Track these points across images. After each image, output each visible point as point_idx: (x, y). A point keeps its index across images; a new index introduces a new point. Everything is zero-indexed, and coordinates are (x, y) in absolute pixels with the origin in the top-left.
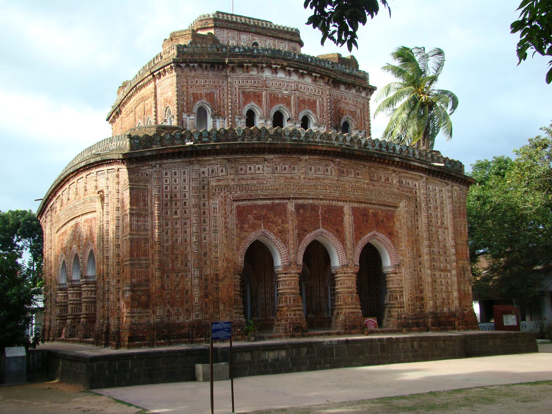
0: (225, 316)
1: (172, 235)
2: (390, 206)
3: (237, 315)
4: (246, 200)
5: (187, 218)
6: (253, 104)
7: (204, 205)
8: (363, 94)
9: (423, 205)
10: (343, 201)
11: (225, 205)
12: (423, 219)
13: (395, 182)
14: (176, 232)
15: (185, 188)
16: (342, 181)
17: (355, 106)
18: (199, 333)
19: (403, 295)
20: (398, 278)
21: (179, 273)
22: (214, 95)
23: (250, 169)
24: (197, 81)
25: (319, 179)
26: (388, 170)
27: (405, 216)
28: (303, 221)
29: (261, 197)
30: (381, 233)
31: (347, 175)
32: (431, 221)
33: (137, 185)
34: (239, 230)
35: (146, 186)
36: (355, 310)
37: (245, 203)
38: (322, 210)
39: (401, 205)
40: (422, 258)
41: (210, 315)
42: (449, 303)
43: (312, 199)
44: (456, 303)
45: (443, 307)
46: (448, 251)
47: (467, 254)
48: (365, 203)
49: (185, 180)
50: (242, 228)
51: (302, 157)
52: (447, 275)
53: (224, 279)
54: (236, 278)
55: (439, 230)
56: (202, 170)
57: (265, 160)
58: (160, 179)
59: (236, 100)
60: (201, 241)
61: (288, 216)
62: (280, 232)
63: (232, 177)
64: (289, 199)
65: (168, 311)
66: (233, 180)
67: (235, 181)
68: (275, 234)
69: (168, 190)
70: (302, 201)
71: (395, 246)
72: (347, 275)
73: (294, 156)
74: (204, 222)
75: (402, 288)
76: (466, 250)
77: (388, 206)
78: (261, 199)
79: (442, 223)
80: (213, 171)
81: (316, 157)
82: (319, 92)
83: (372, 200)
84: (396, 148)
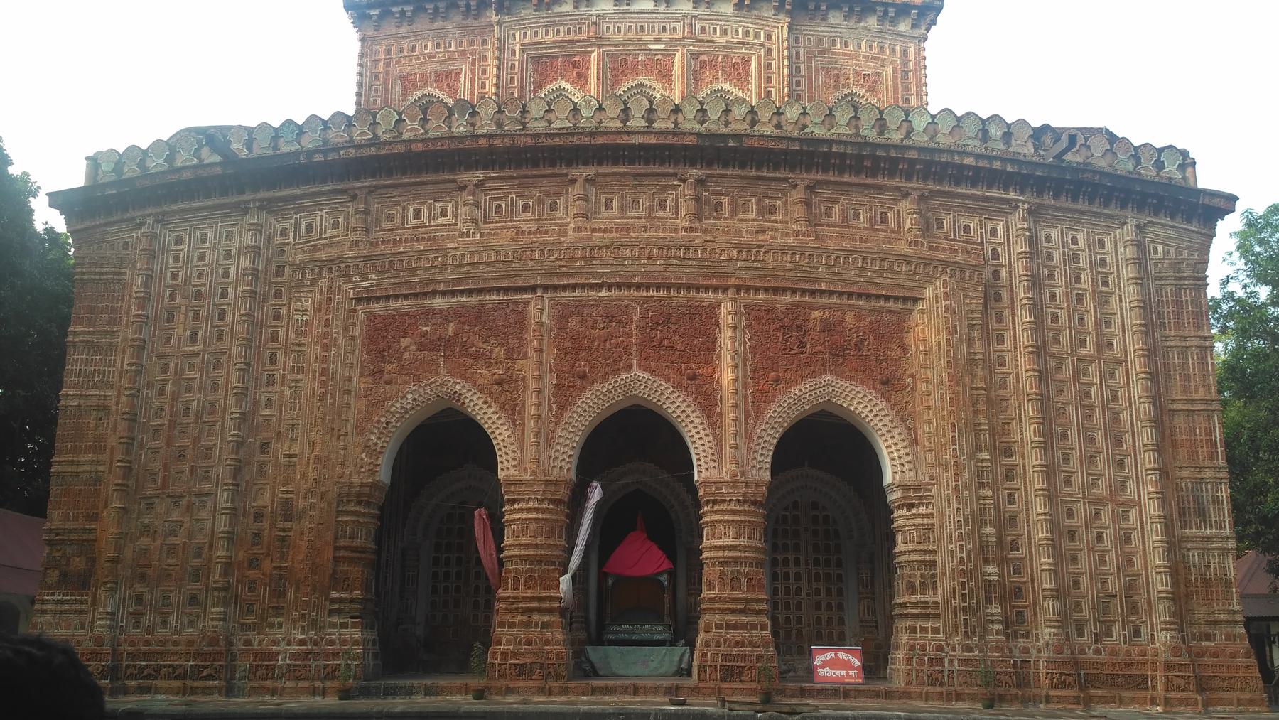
0: (296, 621)
1: (173, 399)
2: (887, 298)
3: (336, 619)
4: (397, 297)
5: (223, 353)
6: (562, 83)
7: (277, 317)
8: (903, 27)
9: (1020, 292)
10: (716, 289)
11: (328, 311)
12: (1019, 336)
13: (908, 225)
14: (188, 390)
15: (226, 274)
16: (706, 231)
17: (874, 59)
18: (205, 667)
19: (934, 576)
20: (919, 521)
21: (181, 496)
22: (458, 74)
23: (418, 214)
24: (414, 47)
25: (627, 229)
26: (880, 189)
27: (942, 325)
28: (576, 350)
29: (441, 287)
30: (852, 379)
31: (733, 213)
32: (1056, 340)
33: (96, 273)
34: (369, 379)
35: (120, 273)
36: (743, 619)
37: (393, 304)
38: (643, 318)
39: (929, 292)
40: (1016, 459)
41: (262, 618)
42: (1134, 610)
43: (610, 286)
44: (1162, 613)
45: (1109, 625)
46: (1128, 436)
47: (1212, 445)
48: (794, 291)
49: (228, 255)
50: (377, 374)
51: (575, 172)
52: (1126, 517)
53: (304, 511)
54: (348, 513)
55: (1092, 368)
56: (279, 227)
57: (464, 188)
58: (151, 255)
59: (512, 80)
60: (255, 409)
61: (529, 337)
62: (499, 383)
63: (352, 236)
64: (533, 289)
65: (139, 600)
66: (356, 244)
67: (362, 245)
68: (481, 389)
69: (179, 282)
70: (577, 293)
71: (903, 420)
72: (723, 507)
73: (550, 171)
74: (273, 359)
75: (933, 552)
76: (1210, 432)
77: (878, 297)
78: (444, 294)
79: (1103, 344)
80: (310, 226)
81: (621, 169)
82: (757, 35)
83: (819, 281)
84: (915, 124)
